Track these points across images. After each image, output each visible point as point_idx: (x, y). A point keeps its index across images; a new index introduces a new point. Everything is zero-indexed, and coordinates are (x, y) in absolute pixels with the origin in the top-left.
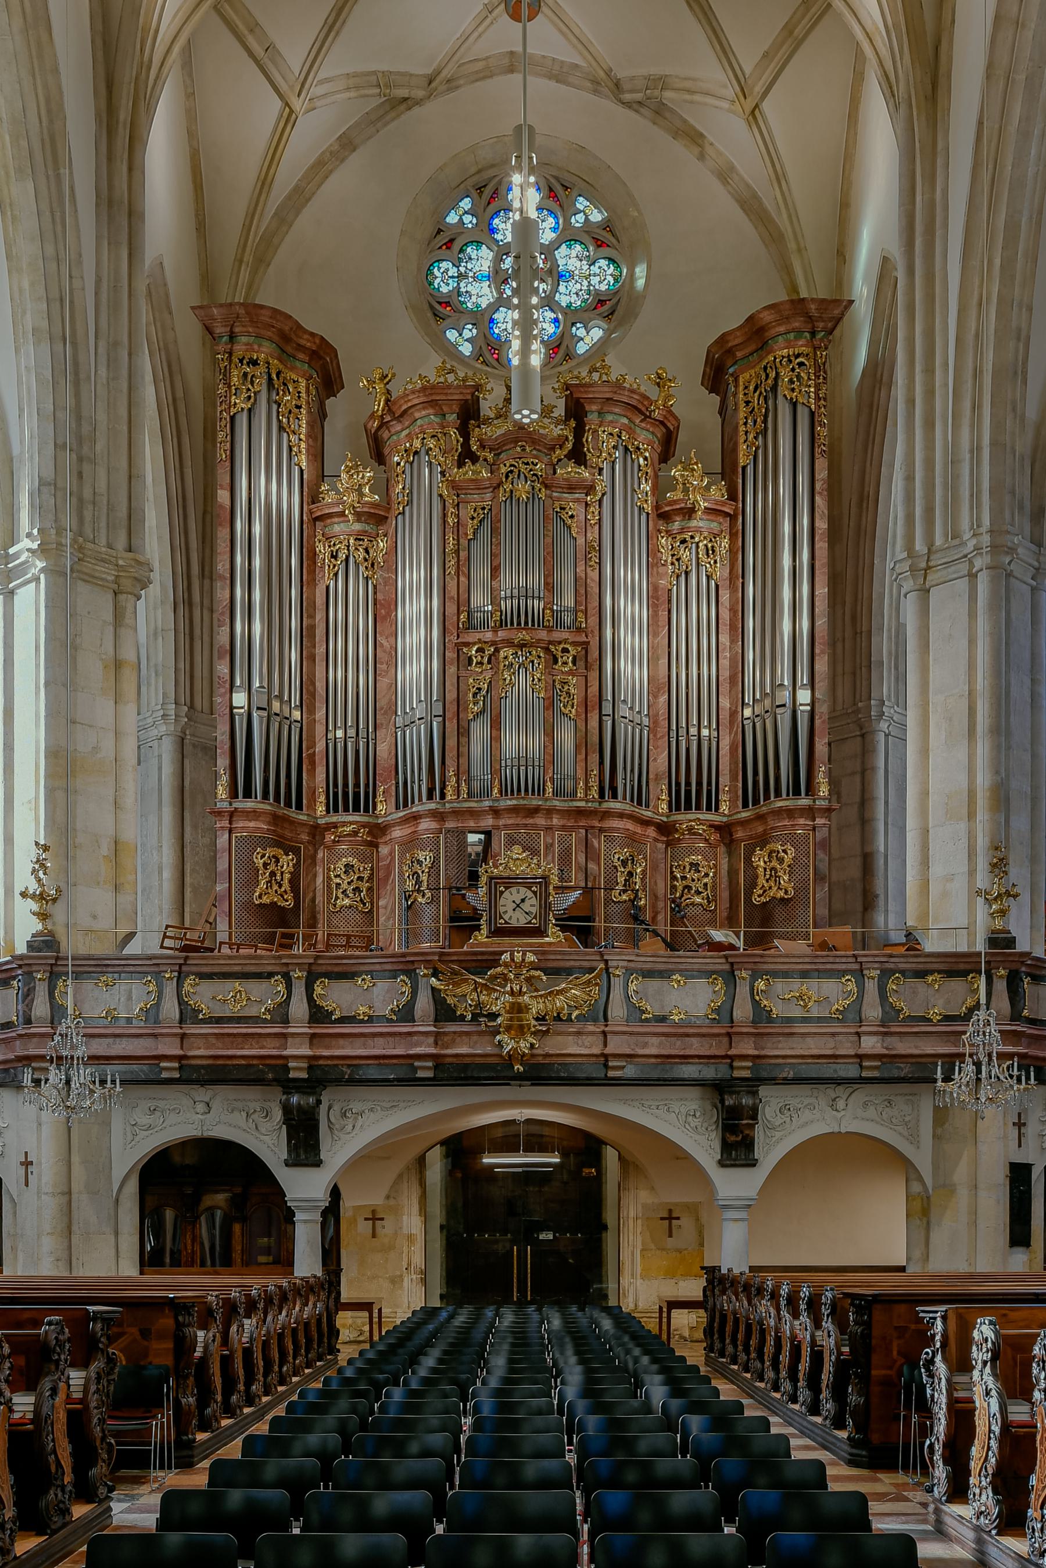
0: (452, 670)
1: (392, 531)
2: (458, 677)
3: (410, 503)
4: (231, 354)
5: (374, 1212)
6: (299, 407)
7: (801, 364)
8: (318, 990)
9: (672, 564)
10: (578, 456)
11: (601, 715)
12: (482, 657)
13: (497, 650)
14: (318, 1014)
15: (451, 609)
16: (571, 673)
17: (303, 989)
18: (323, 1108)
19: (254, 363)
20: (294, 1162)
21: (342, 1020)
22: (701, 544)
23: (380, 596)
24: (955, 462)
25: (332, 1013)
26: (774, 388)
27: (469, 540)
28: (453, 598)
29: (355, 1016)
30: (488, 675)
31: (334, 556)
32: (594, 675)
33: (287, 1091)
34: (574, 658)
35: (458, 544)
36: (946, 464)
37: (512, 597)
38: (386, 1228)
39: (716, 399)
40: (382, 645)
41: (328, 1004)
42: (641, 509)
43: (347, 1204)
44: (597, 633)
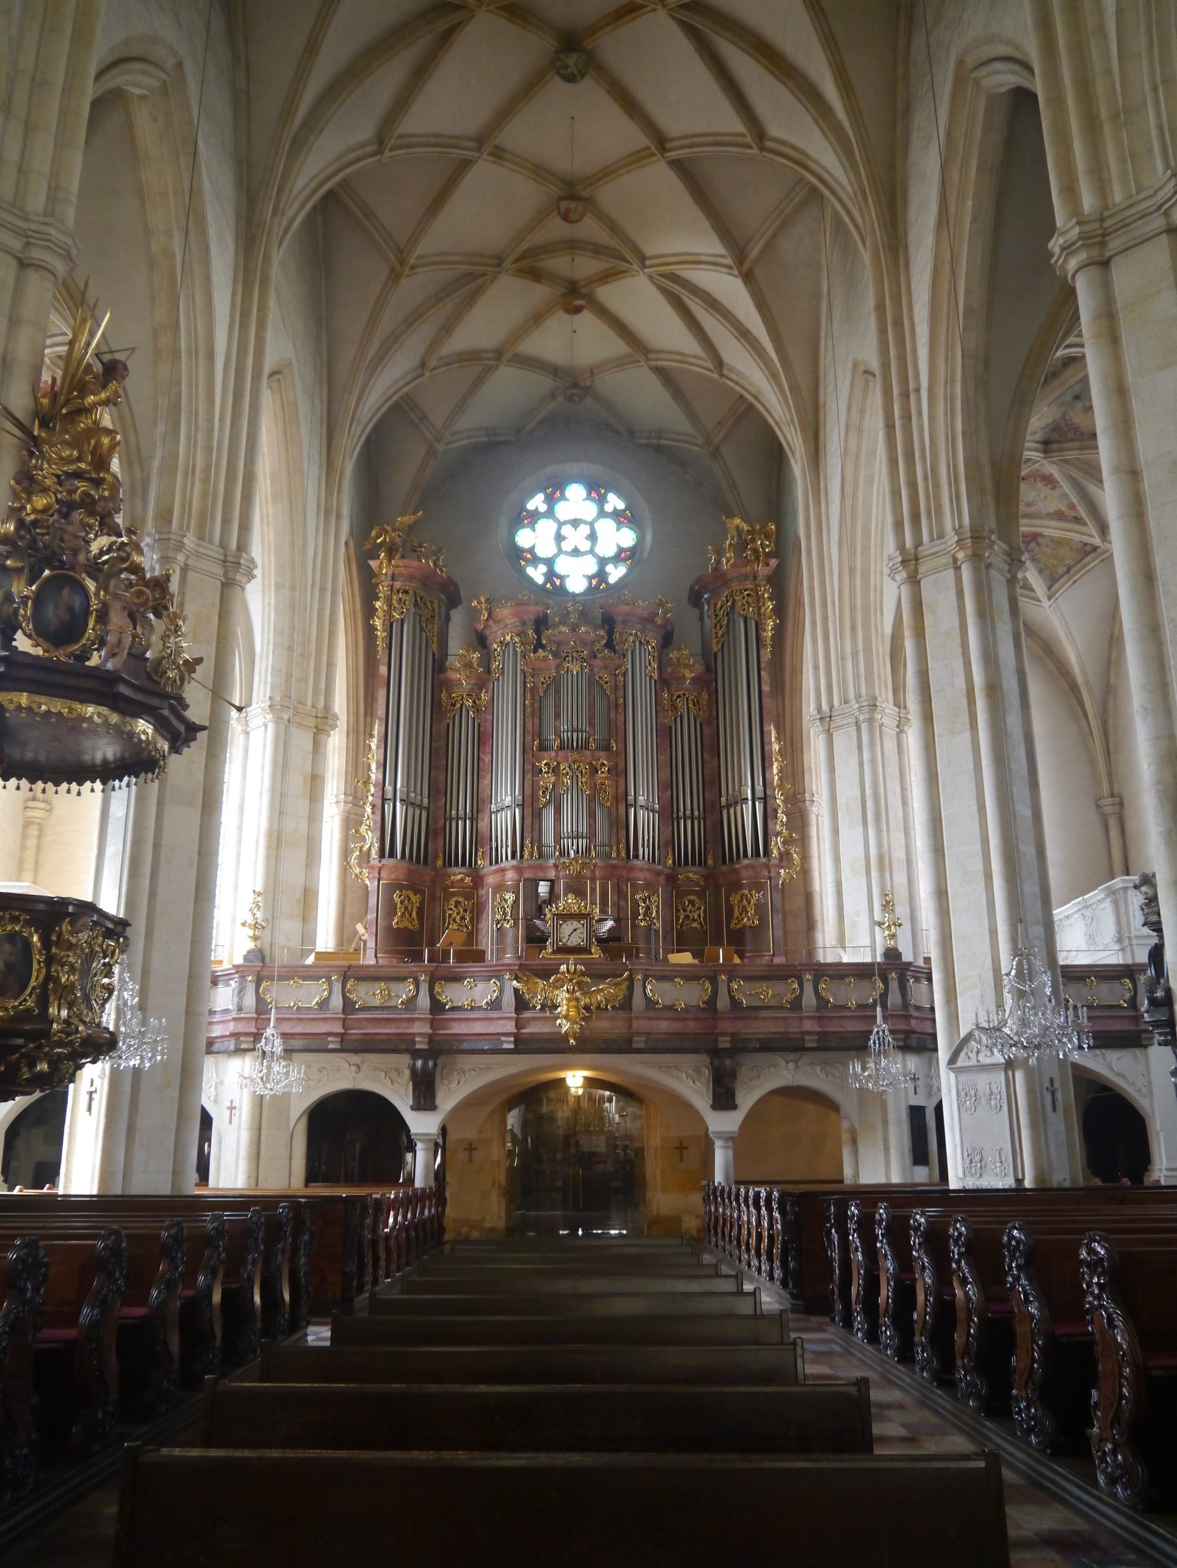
0: (529, 776)
1: (490, 690)
3: (503, 673)
4: (392, 587)
5: (471, 1144)
6: (433, 617)
7: (748, 595)
8: (437, 988)
10: (610, 645)
11: (627, 805)
13: (558, 764)
14: (437, 1007)
15: (529, 738)
16: (606, 778)
18: (438, 1070)
19: (406, 592)
20: (416, 1107)
21: (453, 1009)
24: (843, 659)
26: (733, 607)
30: (553, 779)
31: (454, 705)
33: (414, 1058)
36: (837, 660)
38: (478, 1155)
39: (696, 611)
41: (443, 999)
42: (651, 677)
43: (452, 1136)
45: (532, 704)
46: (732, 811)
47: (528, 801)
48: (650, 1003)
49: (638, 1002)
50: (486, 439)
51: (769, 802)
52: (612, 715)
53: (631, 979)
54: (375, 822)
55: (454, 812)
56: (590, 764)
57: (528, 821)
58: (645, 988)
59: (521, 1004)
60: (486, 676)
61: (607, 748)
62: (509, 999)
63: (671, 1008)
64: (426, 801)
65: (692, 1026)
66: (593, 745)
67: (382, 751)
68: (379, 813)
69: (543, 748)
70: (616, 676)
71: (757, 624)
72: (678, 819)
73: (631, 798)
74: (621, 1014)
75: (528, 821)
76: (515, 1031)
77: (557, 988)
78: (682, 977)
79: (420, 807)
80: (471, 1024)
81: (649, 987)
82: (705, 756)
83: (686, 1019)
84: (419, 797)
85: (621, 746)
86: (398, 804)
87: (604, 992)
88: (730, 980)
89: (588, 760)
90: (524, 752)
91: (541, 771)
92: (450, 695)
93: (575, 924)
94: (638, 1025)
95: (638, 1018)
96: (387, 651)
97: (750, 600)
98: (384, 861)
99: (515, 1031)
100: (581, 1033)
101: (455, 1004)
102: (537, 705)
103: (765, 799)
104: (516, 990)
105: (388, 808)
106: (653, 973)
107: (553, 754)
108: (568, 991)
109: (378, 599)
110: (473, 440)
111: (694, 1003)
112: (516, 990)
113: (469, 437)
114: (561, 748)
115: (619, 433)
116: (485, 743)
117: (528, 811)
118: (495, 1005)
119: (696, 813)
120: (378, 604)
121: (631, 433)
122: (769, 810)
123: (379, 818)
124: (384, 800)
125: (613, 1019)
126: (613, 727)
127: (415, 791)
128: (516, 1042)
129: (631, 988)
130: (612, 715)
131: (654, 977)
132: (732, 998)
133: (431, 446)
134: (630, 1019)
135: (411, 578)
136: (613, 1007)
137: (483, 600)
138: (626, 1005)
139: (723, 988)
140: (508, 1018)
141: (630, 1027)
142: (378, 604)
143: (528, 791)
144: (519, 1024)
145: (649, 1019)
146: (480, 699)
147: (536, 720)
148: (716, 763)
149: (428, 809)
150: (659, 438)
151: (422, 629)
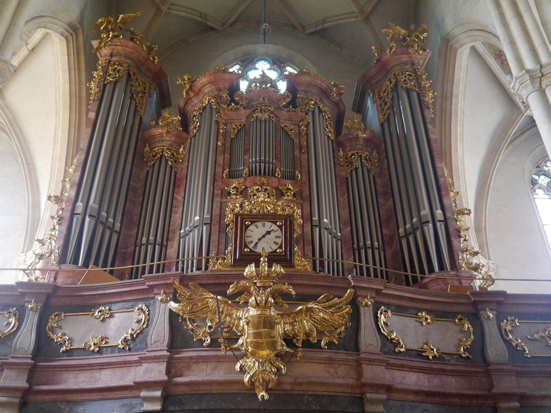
0: (217, 199)
2: (221, 203)
9: (348, 166)
12: (237, 191)
17: (36, 319)
21: (69, 352)
22: (363, 156)
23: (178, 176)
25: (61, 345)
27: (232, 139)
28: (221, 165)
29: (84, 349)
32: (306, 205)
34: (294, 193)
35: (225, 141)
37: (256, 163)
40: (176, 199)
41: (56, 337)
44: (307, 183)
45: (224, 144)
46: (411, 238)
47: (216, 219)
48: (389, 344)
49: (368, 339)
50: (199, 19)
51: (451, 224)
52: (297, 153)
53: (354, 303)
54: (60, 232)
55: (144, 239)
56: (277, 189)
57: (215, 237)
58: (376, 319)
59: (178, 336)
60: (184, 134)
61: (293, 177)
62: (159, 333)
63: (419, 354)
64: (118, 225)
65: (452, 384)
66: (278, 173)
67: (78, 174)
68: (65, 224)
69: (231, 176)
70: (299, 127)
71: (418, 94)
72: (359, 249)
73: (316, 218)
74: (342, 355)
75: (215, 237)
76: (165, 378)
77: (238, 306)
78: (428, 312)
79: (112, 230)
80: (96, 374)
81: (382, 319)
82: (380, 200)
83: (444, 372)
84: (111, 220)
85: (305, 178)
86: (87, 219)
87: (316, 317)
88: (499, 318)
89: (275, 185)
90: (214, 180)
91: (229, 194)
92: (151, 149)
93: (268, 226)
94: (371, 373)
95: (371, 362)
96: (97, 103)
97: (411, 78)
98: (63, 267)
99: (165, 378)
100: (279, 383)
101: (75, 346)
102: (228, 145)
103: (445, 221)
104: (172, 314)
105: (76, 220)
106: (386, 300)
107: (242, 180)
108: (257, 305)
109: (96, 70)
110: (189, 15)
111: (452, 350)
112: (172, 314)
113: (187, 12)
114: (251, 174)
115: (295, 28)
116: (179, 186)
117: (215, 229)
118: (136, 340)
119: (376, 244)
120: (95, 74)
121: (304, 28)
122: (451, 230)
123: (64, 228)
124: (73, 214)
125: (330, 361)
126: (298, 163)
127: (108, 212)
128: (165, 399)
129: (355, 317)
130: (297, 153)
131: (388, 306)
132: (508, 343)
133: (158, 8)
134: (359, 364)
135: (126, 56)
136: (330, 344)
137: (186, 78)
138: (351, 341)
139: (490, 328)
140: (156, 359)
141: (360, 374)
142: (95, 74)
143: (216, 212)
144: (172, 368)
145: (389, 366)
146: (178, 153)
147: (227, 156)
148: (391, 202)
149: (119, 233)
150: (324, 23)
151: (132, 98)
